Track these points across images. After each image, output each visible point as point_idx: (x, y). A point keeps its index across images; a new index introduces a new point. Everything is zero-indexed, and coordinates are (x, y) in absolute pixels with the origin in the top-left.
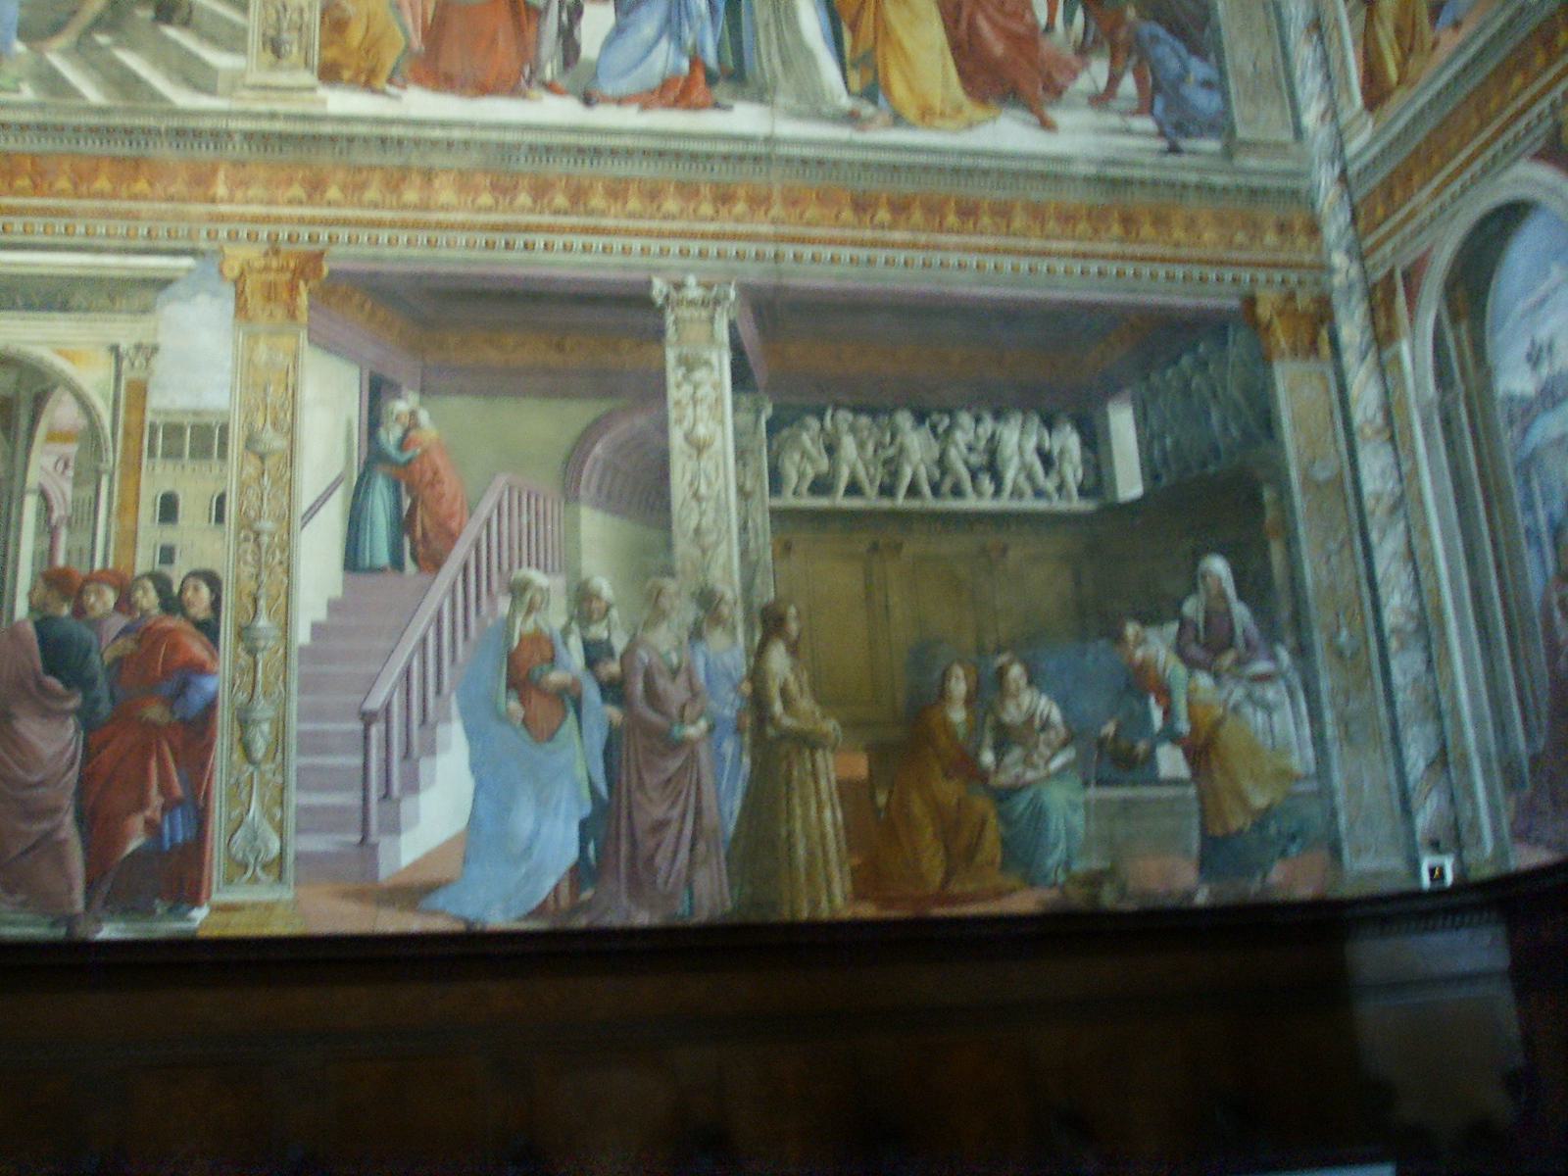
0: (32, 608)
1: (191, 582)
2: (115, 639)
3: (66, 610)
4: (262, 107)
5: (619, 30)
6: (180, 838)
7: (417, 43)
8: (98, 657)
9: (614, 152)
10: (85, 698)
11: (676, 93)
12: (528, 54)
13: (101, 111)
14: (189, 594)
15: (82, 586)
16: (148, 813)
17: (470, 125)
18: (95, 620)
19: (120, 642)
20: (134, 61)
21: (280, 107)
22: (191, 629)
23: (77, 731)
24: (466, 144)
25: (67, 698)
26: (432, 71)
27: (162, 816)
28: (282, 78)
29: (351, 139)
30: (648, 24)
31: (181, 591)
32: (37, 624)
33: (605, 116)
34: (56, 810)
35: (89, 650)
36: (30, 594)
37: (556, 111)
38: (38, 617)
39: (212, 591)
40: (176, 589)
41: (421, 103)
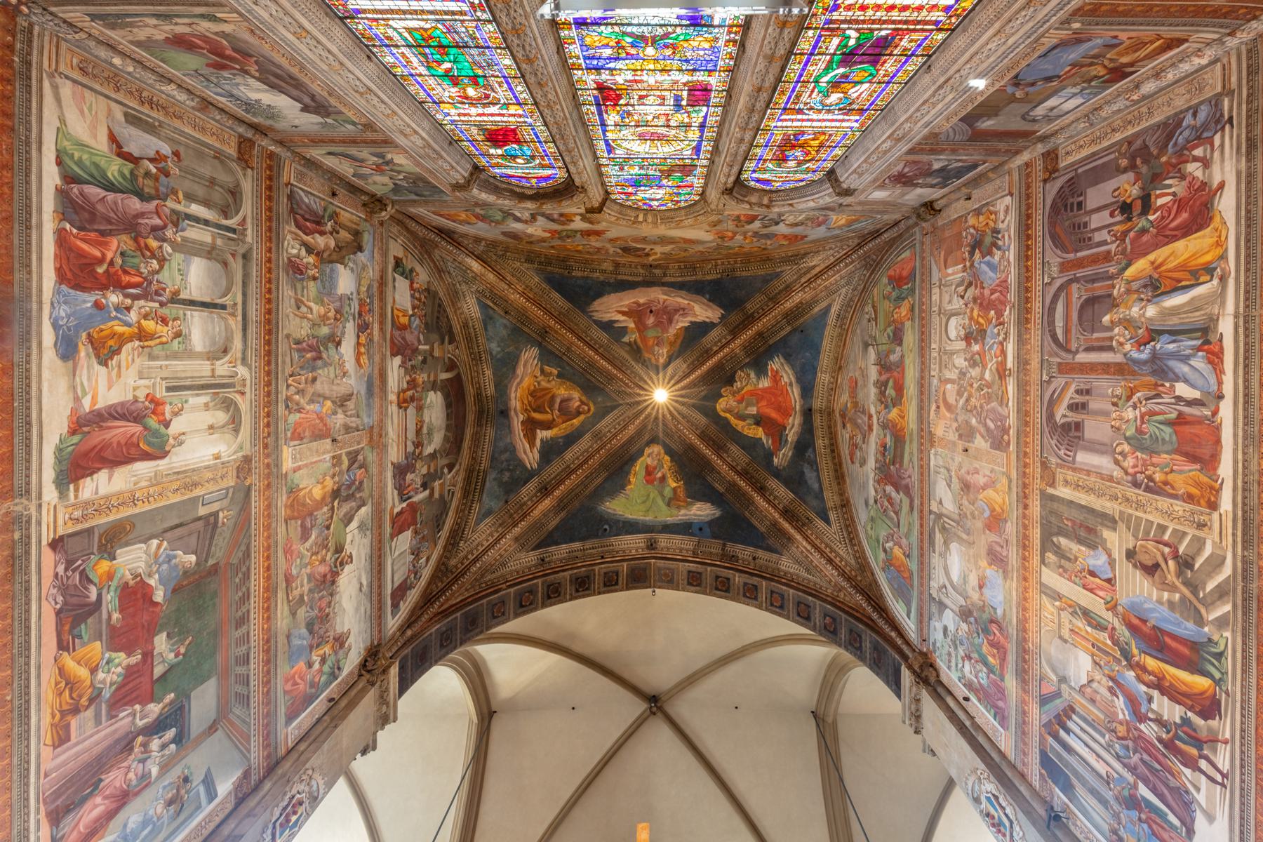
4: (1230, 539)
5: (1186, 381)
7: (1198, 466)
9: (1246, 388)
11: (1215, 358)
12: (1199, 421)
13: (1235, 606)
17: (1235, 451)
20: (1210, 586)
21: (1230, 531)
24: (1244, 453)
26: (1209, 462)
28: (1216, 526)
29: (1244, 504)
30: (1184, 369)
33: (1228, 388)
37: (1226, 411)
41: (1225, 469)
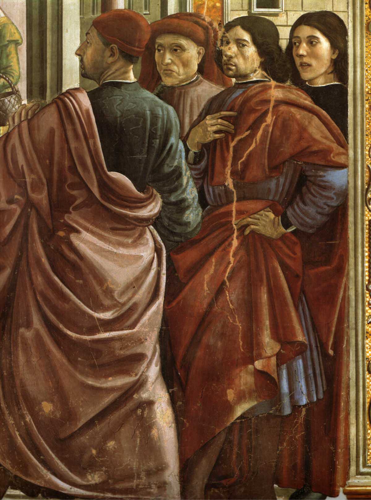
0: (84, 75)
1: (306, 31)
2: (202, 117)
3: (132, 78)
6: (304, 401)
8: (181, 145)
10: (166, 204)
14: (303, 49)
15: (152, 40)
16: (259, 364)
18: (172, 88)
19: (209, 120)
22: (308, 102)
23: (158, 250)
25: (140, 203)
27: (278, 366)
31: (291, 45)
32: (92, 95)
34: (139, 358)
35: (167, 134)
36: (80, 53)
38: (95, 86)
39: (334, 46)
40: (284, 44)
